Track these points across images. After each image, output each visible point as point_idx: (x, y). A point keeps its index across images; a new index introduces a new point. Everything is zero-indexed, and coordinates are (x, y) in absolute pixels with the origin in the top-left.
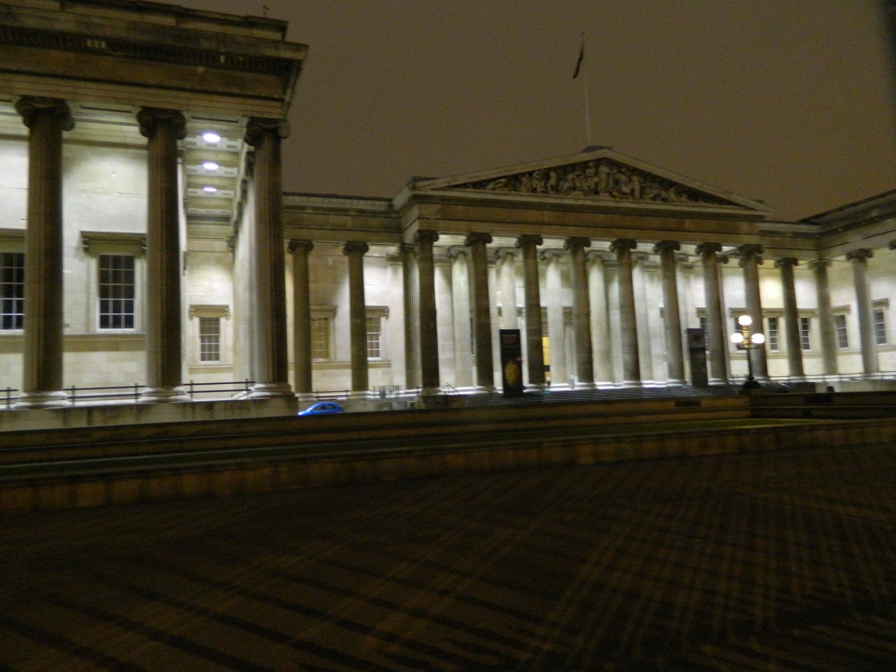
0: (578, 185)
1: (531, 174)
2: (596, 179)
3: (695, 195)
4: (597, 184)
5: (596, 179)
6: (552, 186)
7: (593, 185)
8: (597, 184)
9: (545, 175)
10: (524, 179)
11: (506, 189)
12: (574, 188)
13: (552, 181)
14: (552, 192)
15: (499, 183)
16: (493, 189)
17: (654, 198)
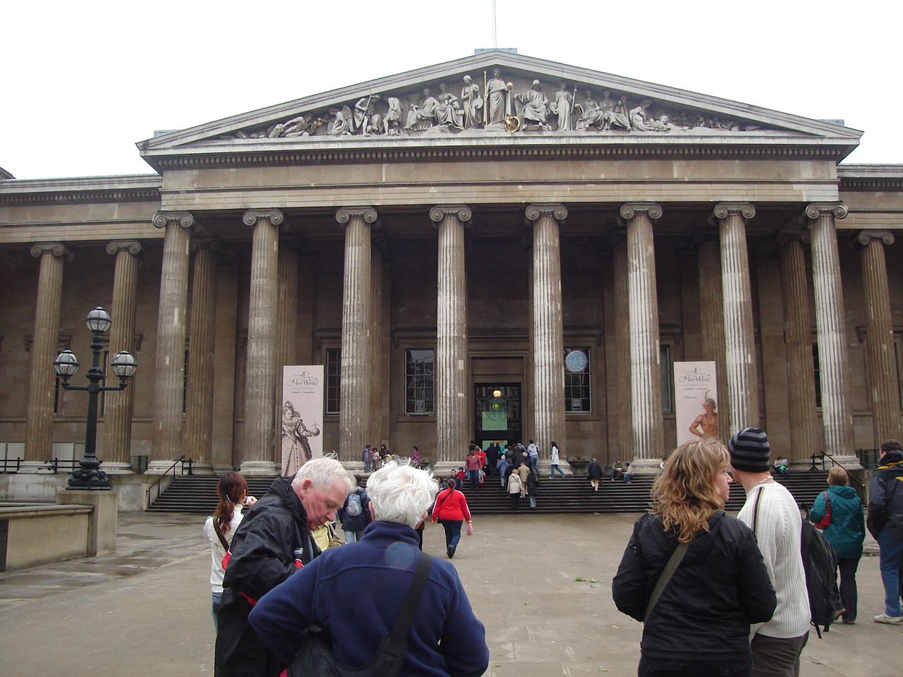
0: (442, 114)
1: (351, 104)
2: (479, 102)
3: (686, 114)
4: (480, 111)
5: (479, 102)
6: (390, 122)
7: (474, 113)
8: (480, 111)
9: (380, 103)
10: (339, 115)
11: (306, 134)
12: (435, 121)
13: (391, 115)
14: (392, 131)
15: (293, 124)
16: (282, 135)
17: (595, 125)
